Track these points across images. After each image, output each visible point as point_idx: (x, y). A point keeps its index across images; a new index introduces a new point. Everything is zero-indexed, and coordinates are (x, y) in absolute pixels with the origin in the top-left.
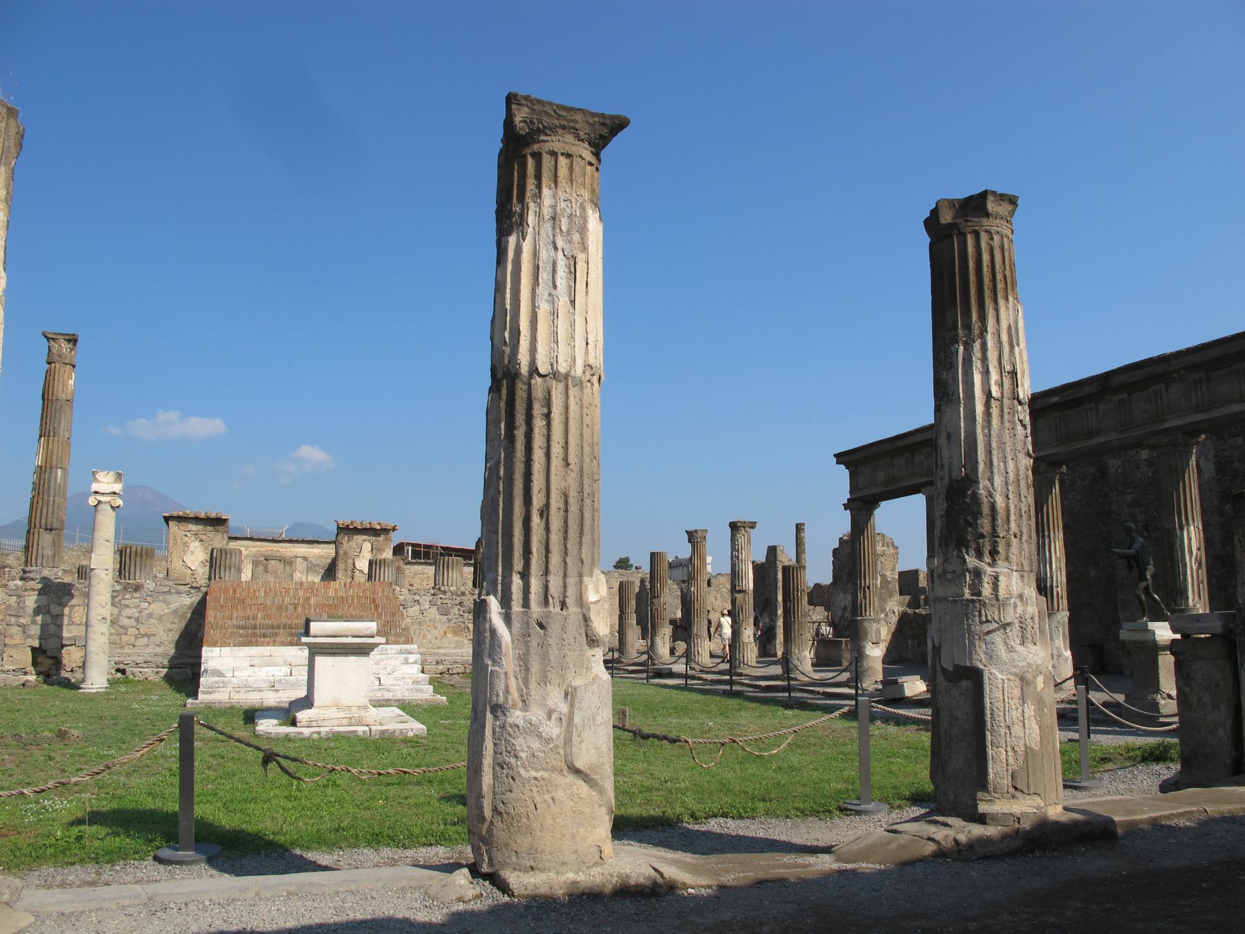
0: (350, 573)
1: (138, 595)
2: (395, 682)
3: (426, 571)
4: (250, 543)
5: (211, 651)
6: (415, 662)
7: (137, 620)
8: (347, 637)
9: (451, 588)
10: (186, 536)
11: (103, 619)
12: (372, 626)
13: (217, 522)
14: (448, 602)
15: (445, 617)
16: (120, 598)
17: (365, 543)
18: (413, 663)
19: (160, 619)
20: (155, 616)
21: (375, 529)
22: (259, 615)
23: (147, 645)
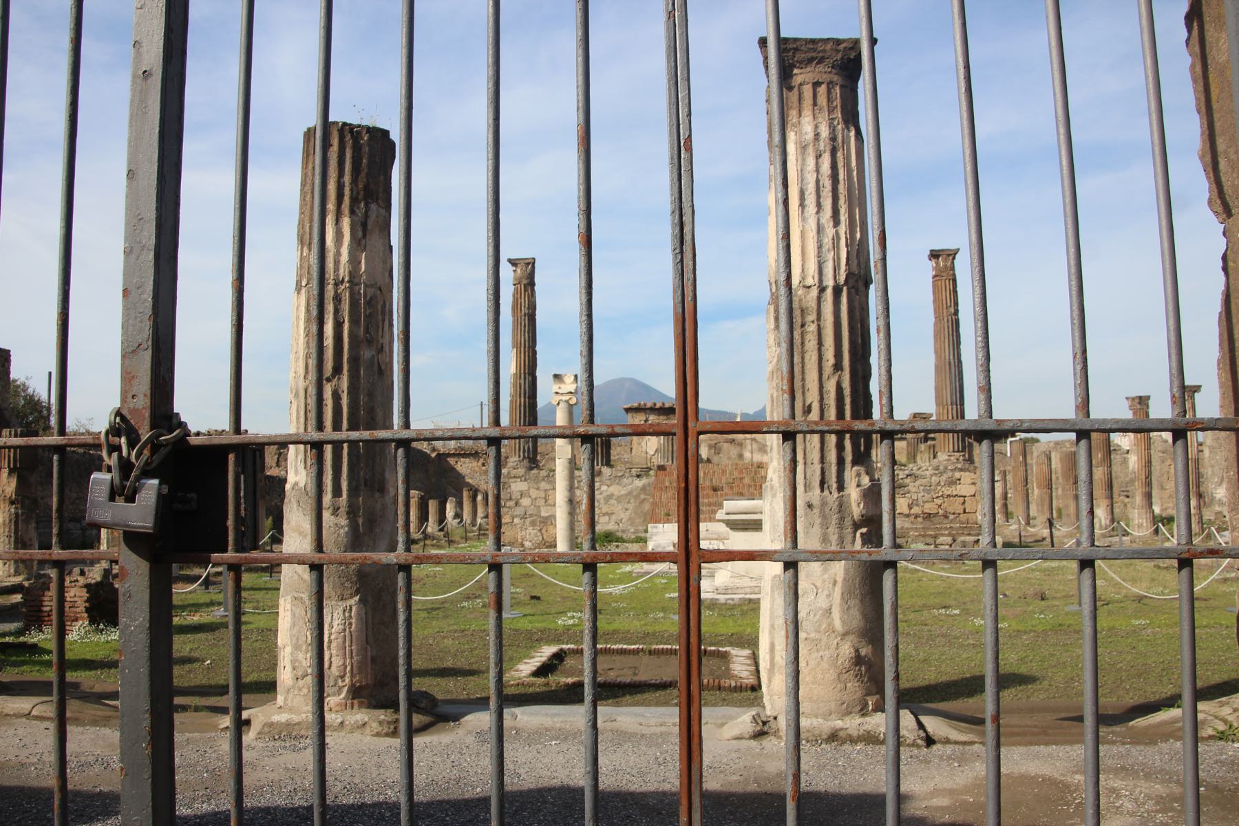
5: (656, 527)
19: (619, 499)
23: (609, 523)
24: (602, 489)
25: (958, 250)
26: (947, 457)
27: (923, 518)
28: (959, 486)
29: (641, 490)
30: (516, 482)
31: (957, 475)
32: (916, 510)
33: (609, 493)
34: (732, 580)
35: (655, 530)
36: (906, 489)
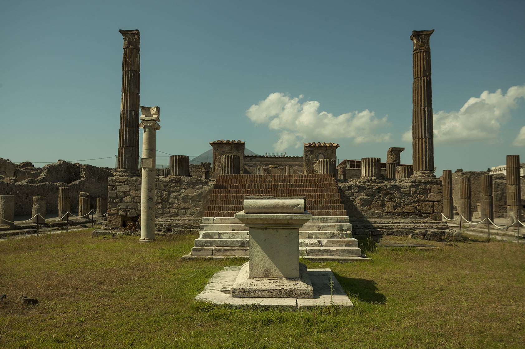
4: (263, 159)
5: (208, 220)
8: (278, 213)
9: (373, 178)
12: (302, 201)
17: (320, 155)
24: (182, 191)
25: (434, 30)
26: (421, 174)
29: (208, 192)
30: (121, 185)
32: (398, 210)
34: (251, 281)
35: (207, 222)
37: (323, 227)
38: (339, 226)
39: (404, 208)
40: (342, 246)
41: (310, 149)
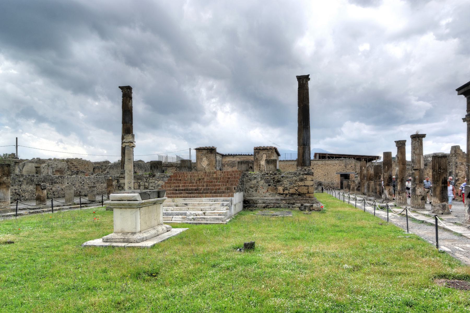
0: (259, 166)
1: (154, 178)
2: (211, 215)
3: (318, 163)
4: (241, 157)
6: (226, 206)
7: (154, 187)
9: (270, 172)
10: (201, 156)
11: (130, 188)
13: (212, 150)
14: (268, 177)
15: (267, 184)
16: (148, 179)
17: (264, 154)
18: (226, 206)
20: (160, 186)
21: (268, 149)
22: (181, 186)
24: (156, 182)
26: (301, 169)
27: (289, 195)
28: (305, 182)
31: (305, 176)
32: (286, 192)
33: (158, 184)
36: (281, 183)
37: (213, 204)
38: (221, 204)
39: (289, 190)
40: (216, 216)
41: (257, 151)
